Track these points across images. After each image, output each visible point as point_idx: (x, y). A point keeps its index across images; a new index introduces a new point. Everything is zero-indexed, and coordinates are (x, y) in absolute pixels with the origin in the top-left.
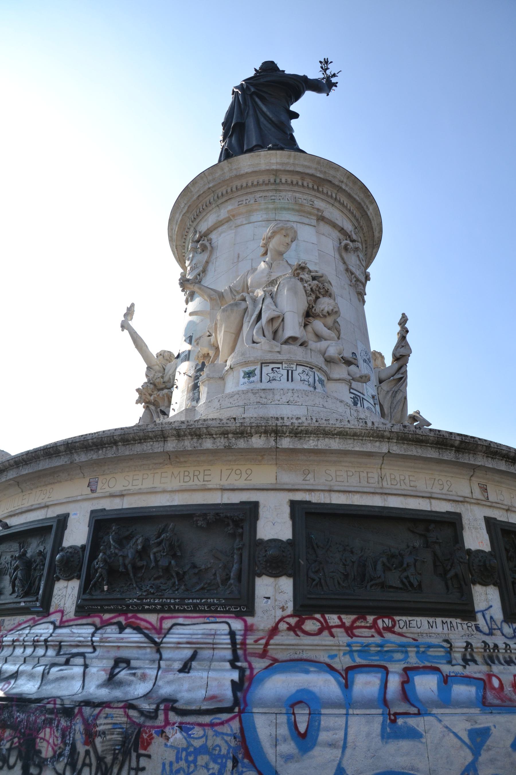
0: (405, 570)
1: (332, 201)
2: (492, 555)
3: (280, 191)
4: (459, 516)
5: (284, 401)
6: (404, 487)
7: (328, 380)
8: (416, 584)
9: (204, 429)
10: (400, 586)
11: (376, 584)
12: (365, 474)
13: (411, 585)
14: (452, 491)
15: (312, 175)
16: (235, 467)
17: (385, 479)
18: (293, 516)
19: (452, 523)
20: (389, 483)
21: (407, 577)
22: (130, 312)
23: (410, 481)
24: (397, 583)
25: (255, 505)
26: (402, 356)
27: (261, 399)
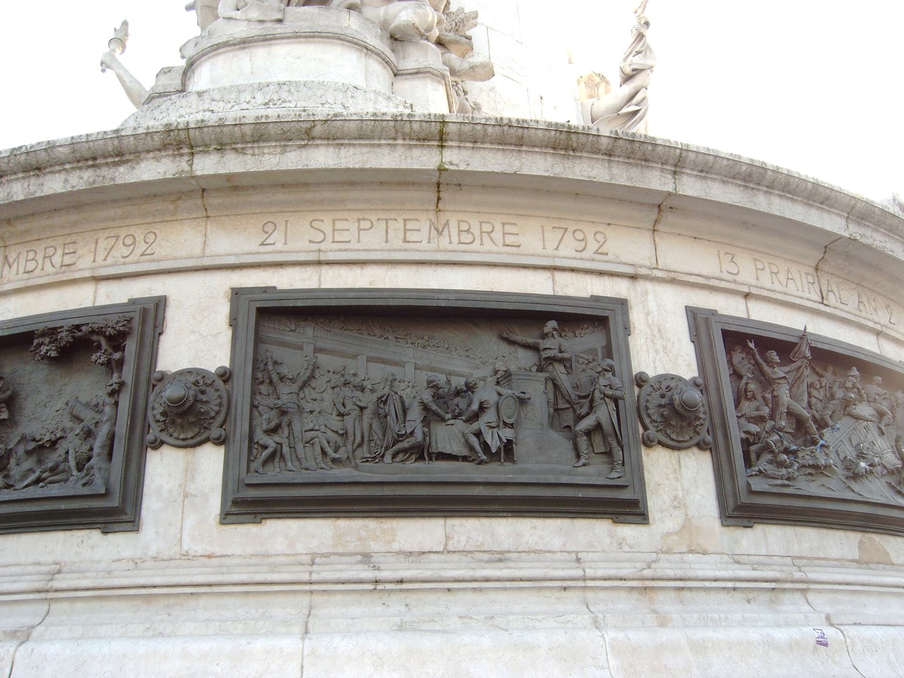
0: (476, 416)
2: (697, 385)
4: (623, 304)
5: (259, 102)
7: (395, 75)
8: (494, 445)
9: (43, 153)
10: (465, 452)
11: (405, 451)
12: (400, 224)
13: (486, 447)
14: (607, 254)
16: (123, 232)
17: (446, 232)
19: (599, 321)
20: (455, 239)
21: (478, 434)
22: (120, 39)
23: (504, 234)
24: (457, 448)
25: (160, 304)
26: (637, 72)
27: (213, 103)
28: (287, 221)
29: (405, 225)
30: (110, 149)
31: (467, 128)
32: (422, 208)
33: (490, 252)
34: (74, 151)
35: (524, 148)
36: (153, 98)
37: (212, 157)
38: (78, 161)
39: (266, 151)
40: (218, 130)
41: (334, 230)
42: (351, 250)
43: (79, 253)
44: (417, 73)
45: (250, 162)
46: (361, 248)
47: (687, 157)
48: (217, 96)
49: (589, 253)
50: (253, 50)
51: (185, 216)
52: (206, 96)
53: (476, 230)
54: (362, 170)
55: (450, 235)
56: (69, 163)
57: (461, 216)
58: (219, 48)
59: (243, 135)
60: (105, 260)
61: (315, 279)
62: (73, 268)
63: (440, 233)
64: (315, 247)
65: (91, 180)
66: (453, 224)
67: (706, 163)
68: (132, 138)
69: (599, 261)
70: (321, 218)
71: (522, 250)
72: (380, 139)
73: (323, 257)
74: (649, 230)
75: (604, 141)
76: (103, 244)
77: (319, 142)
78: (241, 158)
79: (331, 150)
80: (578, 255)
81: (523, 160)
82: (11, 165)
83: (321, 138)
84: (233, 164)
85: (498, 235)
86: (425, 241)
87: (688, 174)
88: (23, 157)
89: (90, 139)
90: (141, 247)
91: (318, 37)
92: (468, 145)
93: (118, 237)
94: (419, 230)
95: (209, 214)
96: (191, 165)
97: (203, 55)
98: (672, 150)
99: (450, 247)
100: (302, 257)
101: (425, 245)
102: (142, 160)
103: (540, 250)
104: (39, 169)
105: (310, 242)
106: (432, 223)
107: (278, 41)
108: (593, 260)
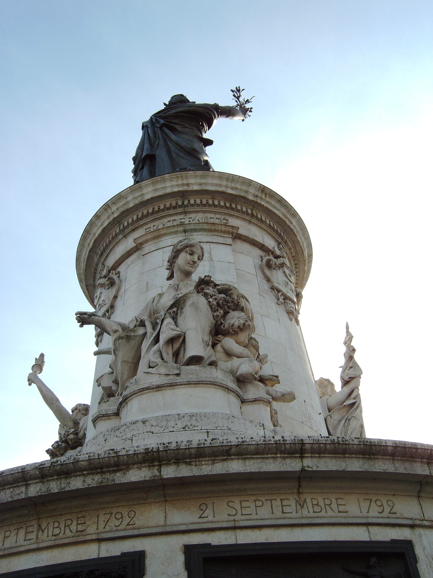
1: (248, 218)
3: (190, 212)
4: (409, 544)
5: (180, 427)
6: (330, 513)
9: (71, 465)
12: (279, 503)
14: (396, 513)
15: (223, 193)
16: (115, 511)
17: (305, 506)
18: (188, 566)
20: (311, 510)
22: (39, 364)
23: (338, 505)
25: (140, 556)
26: (351, 379)
27: (153, 427)
28: (213, 503)
29: (282, 503)
30: (112, 463)
31: (316, 446)
32: (290, 492)
33: (331, 517)
34: (90, 464)
35: (347, 456)
36: (99, 417)
37: (172, 467)
38: (92, 470)
39: (203, 463)
40: (176, 452)
41: (241, 507)
42: (253, 520)
43: (87, 523)
44: (255, 401)
45: (194, 470)
46: (258, 518)
48: (155, 424)
49: (386, 514)
50: (163, 391)
51: (152, 500)
52: (147, 423)
53: (321, 503)
54: (259, 473)
55: (308, 508)
56: (86, 470)
57: (312, 496)
58: (144, 390)
59: (191, 454)
60: (104, 528)
61: (233, 537)
62: (84, 533)
63: (302, 507)
64: (232, 518)
65: (100, 481)
66: (309, 501)
68: (125, 457)
69: (392, 518)
70: (232, 500)
71: (349, 514)
72: (267, 454)
73: (237, 525)
74: (415, 496)
75: (390, 448)
76: (102, 518)
77: (233, 457)
78: (189, 467)
79: (240, 461)
80: (380, 515)
81: (347, 463)
82: (51, 472)
83: (234, 455)
84: (185, 471)
85: (334, 506)
86: (294, 512)
88: (59, 467)
89: (100, 457)
90: (127, 520)
92: (316, 455)
93: (111, 514)
94: (290, 506)
95: (167, 499)
96: (160, 472)
97: (133, 394)
99: (309, 515)
100: (225, 525)
101: (294, 515)
102: (130, 469)
103: (359, 514)
104: (67, 474)
105: (229, 515)
106: (297, 501)
107: (178, 387)
108: (389, 518)
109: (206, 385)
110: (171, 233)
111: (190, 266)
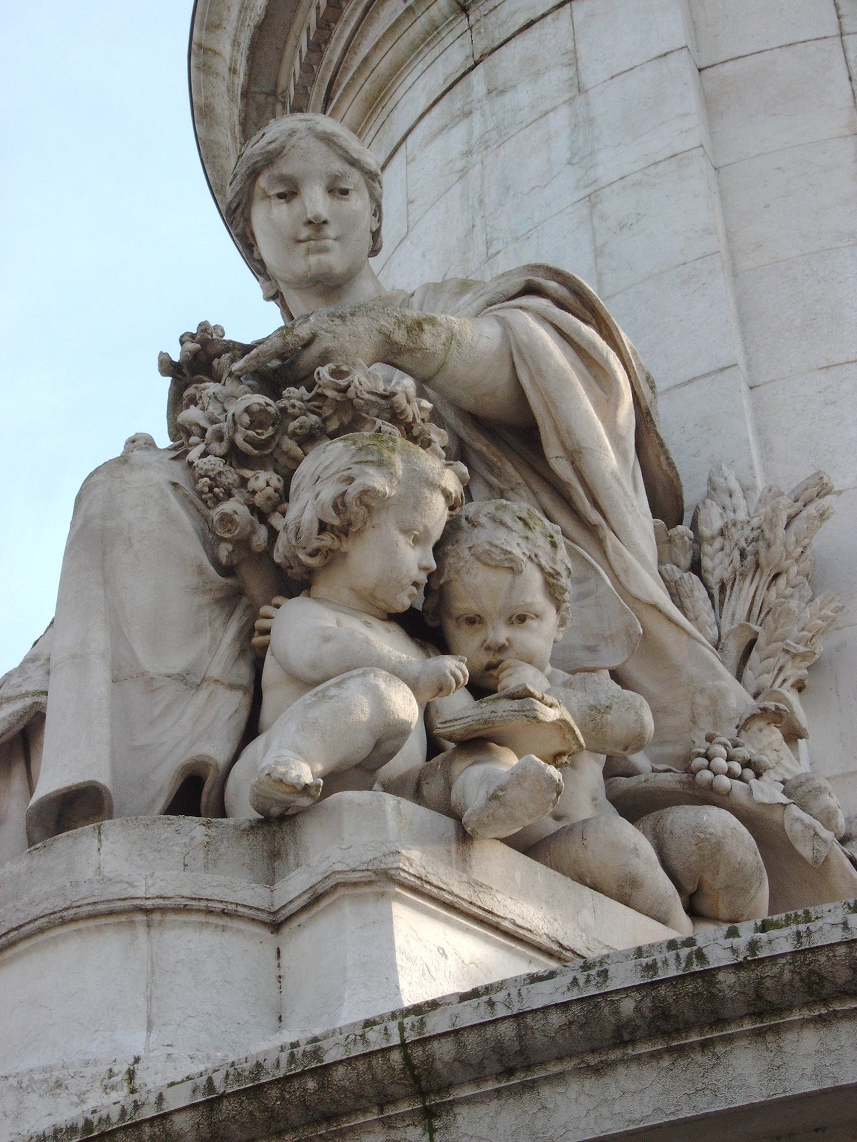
44: (316, 898)
47: (430, 1060)
67: (499, 1048)
75: (182, 1123)
87: (468, 1101)
91: (22, 939)
98: (378, 1062)
109: (41, 938)
110: (416, 49)
111: (308, 252)
